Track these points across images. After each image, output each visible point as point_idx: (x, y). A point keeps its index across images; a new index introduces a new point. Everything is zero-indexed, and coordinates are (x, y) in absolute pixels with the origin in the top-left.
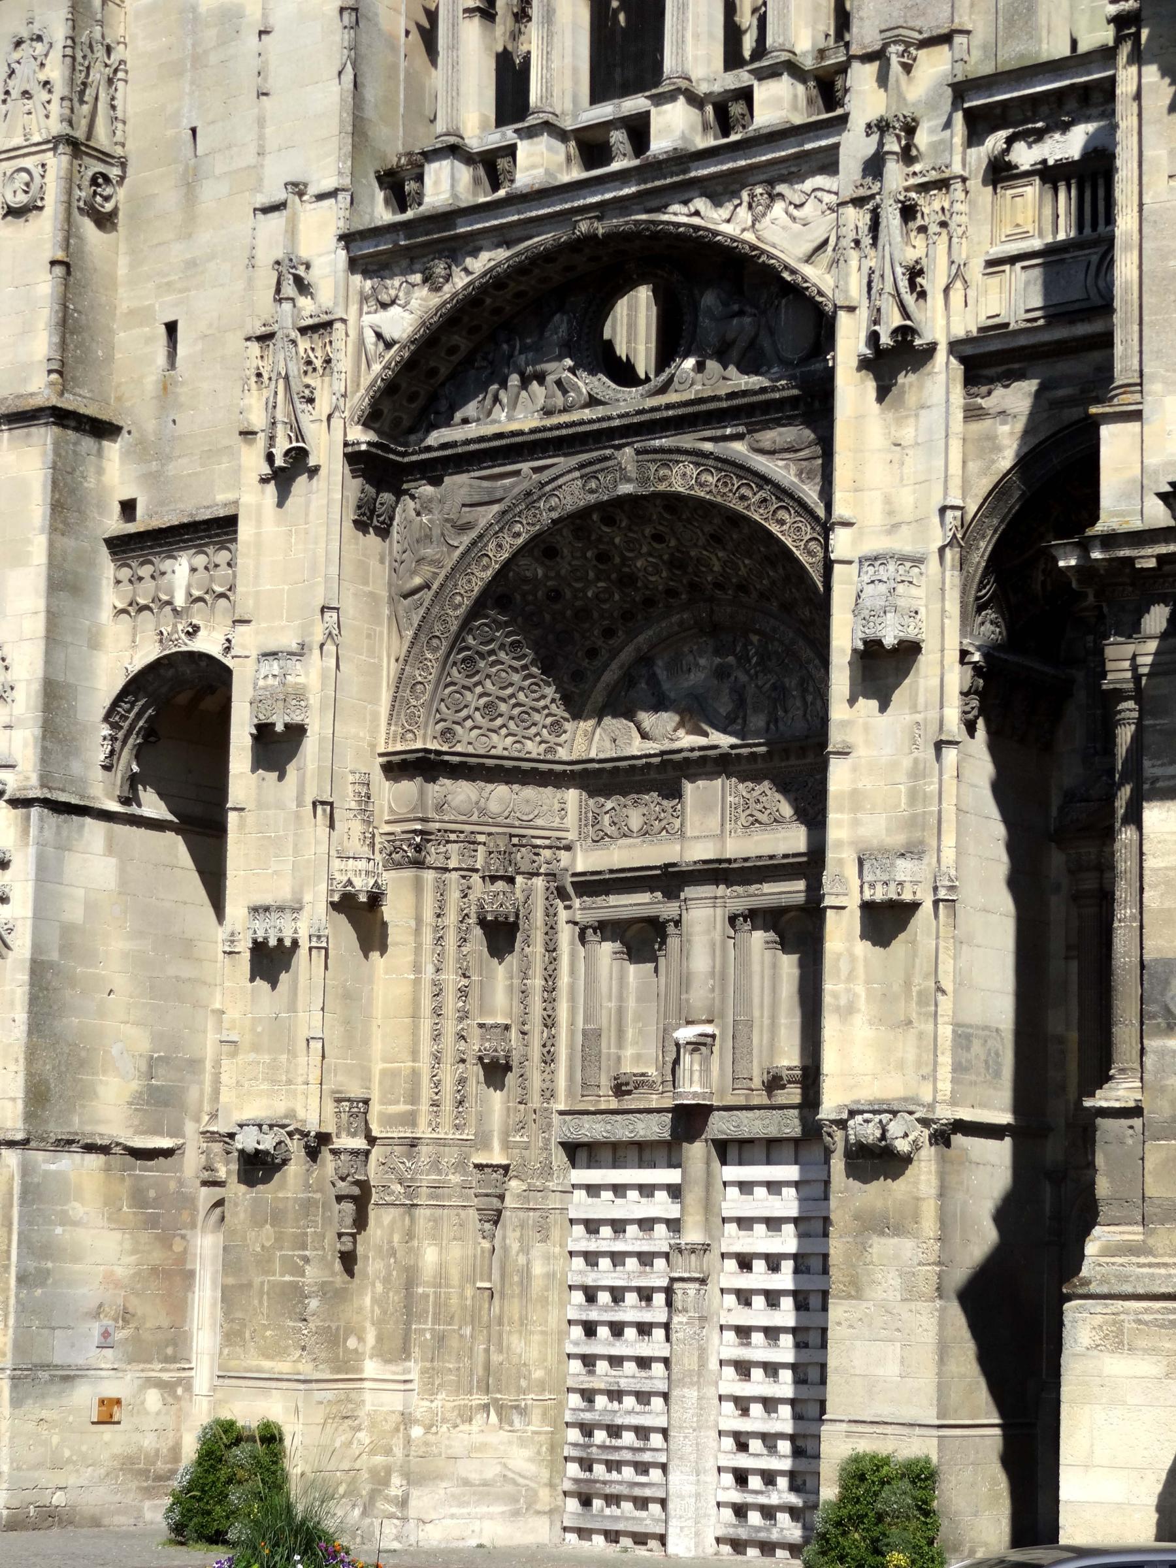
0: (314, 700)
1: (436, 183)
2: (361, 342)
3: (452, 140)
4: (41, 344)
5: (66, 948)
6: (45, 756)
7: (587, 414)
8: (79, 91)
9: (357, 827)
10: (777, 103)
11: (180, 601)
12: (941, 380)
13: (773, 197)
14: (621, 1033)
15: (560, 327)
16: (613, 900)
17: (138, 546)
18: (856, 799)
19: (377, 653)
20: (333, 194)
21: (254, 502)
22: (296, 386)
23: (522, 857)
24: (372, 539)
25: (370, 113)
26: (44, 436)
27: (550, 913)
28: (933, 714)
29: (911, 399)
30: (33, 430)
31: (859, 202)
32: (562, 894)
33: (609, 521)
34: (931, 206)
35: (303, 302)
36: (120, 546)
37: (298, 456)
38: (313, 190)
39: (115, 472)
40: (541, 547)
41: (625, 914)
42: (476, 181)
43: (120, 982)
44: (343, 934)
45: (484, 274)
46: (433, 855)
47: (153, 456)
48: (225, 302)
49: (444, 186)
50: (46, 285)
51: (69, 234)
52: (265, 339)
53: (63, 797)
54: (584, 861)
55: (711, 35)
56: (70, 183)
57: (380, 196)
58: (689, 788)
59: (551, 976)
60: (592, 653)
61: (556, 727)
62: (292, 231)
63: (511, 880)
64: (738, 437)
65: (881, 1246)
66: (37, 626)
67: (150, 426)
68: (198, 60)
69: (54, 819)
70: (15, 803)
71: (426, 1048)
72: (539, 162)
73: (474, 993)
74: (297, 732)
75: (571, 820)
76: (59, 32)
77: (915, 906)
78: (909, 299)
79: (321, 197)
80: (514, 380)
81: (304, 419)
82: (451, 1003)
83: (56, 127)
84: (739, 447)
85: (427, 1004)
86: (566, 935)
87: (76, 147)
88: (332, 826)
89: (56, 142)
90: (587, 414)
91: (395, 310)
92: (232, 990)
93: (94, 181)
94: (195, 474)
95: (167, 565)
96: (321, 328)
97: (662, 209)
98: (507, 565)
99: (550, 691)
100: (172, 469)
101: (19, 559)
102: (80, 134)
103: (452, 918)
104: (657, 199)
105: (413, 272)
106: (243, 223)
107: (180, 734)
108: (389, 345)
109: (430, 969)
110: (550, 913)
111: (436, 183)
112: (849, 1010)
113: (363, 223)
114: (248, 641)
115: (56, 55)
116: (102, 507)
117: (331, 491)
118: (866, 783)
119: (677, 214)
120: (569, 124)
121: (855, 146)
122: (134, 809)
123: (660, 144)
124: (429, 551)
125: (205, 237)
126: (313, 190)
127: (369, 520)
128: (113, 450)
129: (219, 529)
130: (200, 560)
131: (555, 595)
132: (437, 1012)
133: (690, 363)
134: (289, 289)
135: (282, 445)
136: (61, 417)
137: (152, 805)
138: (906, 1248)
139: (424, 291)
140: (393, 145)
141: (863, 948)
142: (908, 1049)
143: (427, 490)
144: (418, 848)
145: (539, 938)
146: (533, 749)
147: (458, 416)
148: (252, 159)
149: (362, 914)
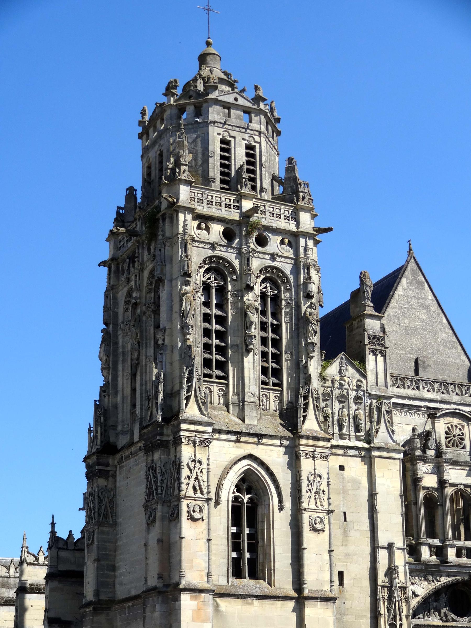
1: (425, 552)
30: (329, 603)
45: (444, 583)
91: (415, 585)
94: (355, 622)
100: (345, 618)
105: (421, 577)
108: (416, 595)
111: (425, 552)
126: (396, 546)
147: (417, 617)
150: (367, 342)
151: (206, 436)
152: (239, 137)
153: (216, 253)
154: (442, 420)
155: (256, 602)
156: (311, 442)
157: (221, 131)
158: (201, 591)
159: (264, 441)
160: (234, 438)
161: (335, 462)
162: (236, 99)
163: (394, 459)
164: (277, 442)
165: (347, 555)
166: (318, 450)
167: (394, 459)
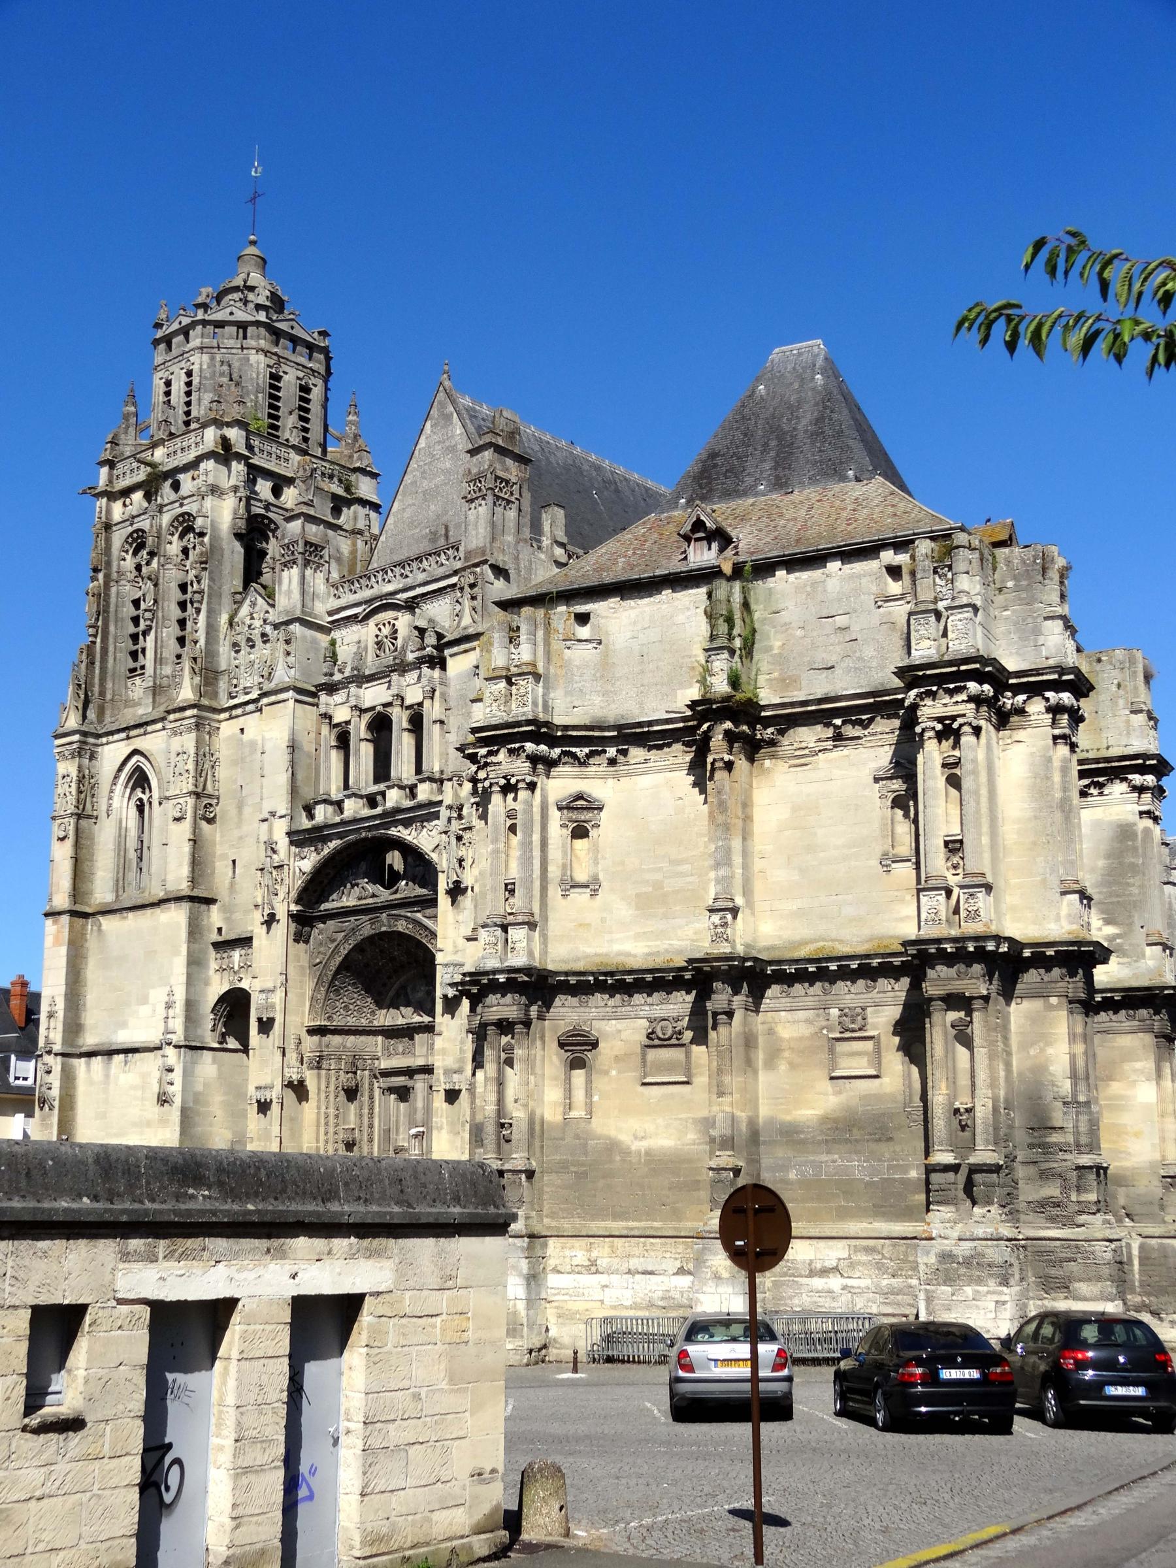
0: (278, 1008)
2: (294, 872)
3: (325, 797)
4: (185, 871)
5: (196, 1100)
6: (186, 1029)
7: (371, 901)
8: (199, 772)
9: (294, 1055)
10: (424, 792)
11: (236, 968)
13: (423, 827)
14: (397, 1130)
15: (363, 866)
16: (393, 1079)
17: (223, 946)
18: (444, 1052)
19: (305, 987)
20: (284, 816)
21: (258, 931)
22: (271, 889)
23: (360, 1063)
24: (302, 945)
25: (299, 783)
26: (186, 906)
27: (371, 1084)
29: (462, 905)
31: (446, 833)
32: (376, 1077)
33: (381, 939)
34: (467, 836)
35: (275, 856)
36: (217, 946)
38: (278, 814)
39: (215, 917)
40: (359, 948)
41: (396, 1085)
42: (335, 811)
43: (219, 1112)
44: (290, 1096)
46: (325, 1064)
47: (227, 910)
48: (251, 855)
49: (322, 814)
50: (187, 848)
51: (195, 827)
52: (262, 870)
53: (194, 1044)
55: (409, 762)
56: (196, 809)
57: (304, 814)
58: (417, 1037)
59: (371, 1108)
60: (384, 985)
61: (373, 1013)
62: (270, 830)
63: (355, 1073)
64: (418, 911)
66: (184, 979)
67: (227, 899)
68: (243, 759)
69: (190, 1052)
70: (176, 1047)
71: (322, 1137)
72: (352, 808)
73: (341, 1116)
74: (271, 1021)
75: (379, 1048)
76: (192, 751)
77: (460, 1091)
78: (458, 870)
79: (281, 817)
80: (349, 886)
81: (274, 902)
82: (332, 1120)
83: (191, 788)
84: (419, 915)
85: (322, 1121)
86: (377, 1092)
87: (198, 795)
88: (284, 1055)
89: (191, 793)
90: (371, 901)
92: (253, 1119)
93: (205, 807)
96: (280, 867)
97: (388, 829)
98: (347, 956)
99: (369, 1000)
100: (234, 917)
101: (177, 953)
102: (199, 790)
103: (332, 1088)
104: (387, 826)
106: (256, 824)
109: (323, 1109)
110: (371, 1084)
112: (440, 1129)
113: (295, 828)
115: (191, 759)
116: (210, 931)
117: (282, 928)
118: (446, 1045)
119: (393, 831)
120: (363, 793)
121: (444, 813)
122: (225, 1046)
123: (390, 804)
124: (322, 949)
125: (246, 828)
126: (278, 814)
127: (299, 937)
128: (214, 908)
129: (245, 942)
130: (243, 952)
131: (367, 965)
132: (326, 1124)
133: (404, 882)
134: (269, 853)
135: (267, 912)
136: (192, 899)
137: (232, 1043)
139: (314, 854)
140: (308, 794)
141: (445, 1105)
142: (458, 1143)
143: (322, 925)
144: (318, 1062)
145: (366, 1094)
146: (364, 1022)
148: (258, 800)
149: (299, 1090)
151: (75, 746)
152: (175, 368)
153: (135, 526)
154: (372, 622)
155: (131, 915)
156: (178, 715)
158: (60, 913)
159: (149, 728)
160: (123, 735)
161: (235, 725)
163: (284, 701)
164: (159, 726)
166: (185, 722)
167: (284, 701)
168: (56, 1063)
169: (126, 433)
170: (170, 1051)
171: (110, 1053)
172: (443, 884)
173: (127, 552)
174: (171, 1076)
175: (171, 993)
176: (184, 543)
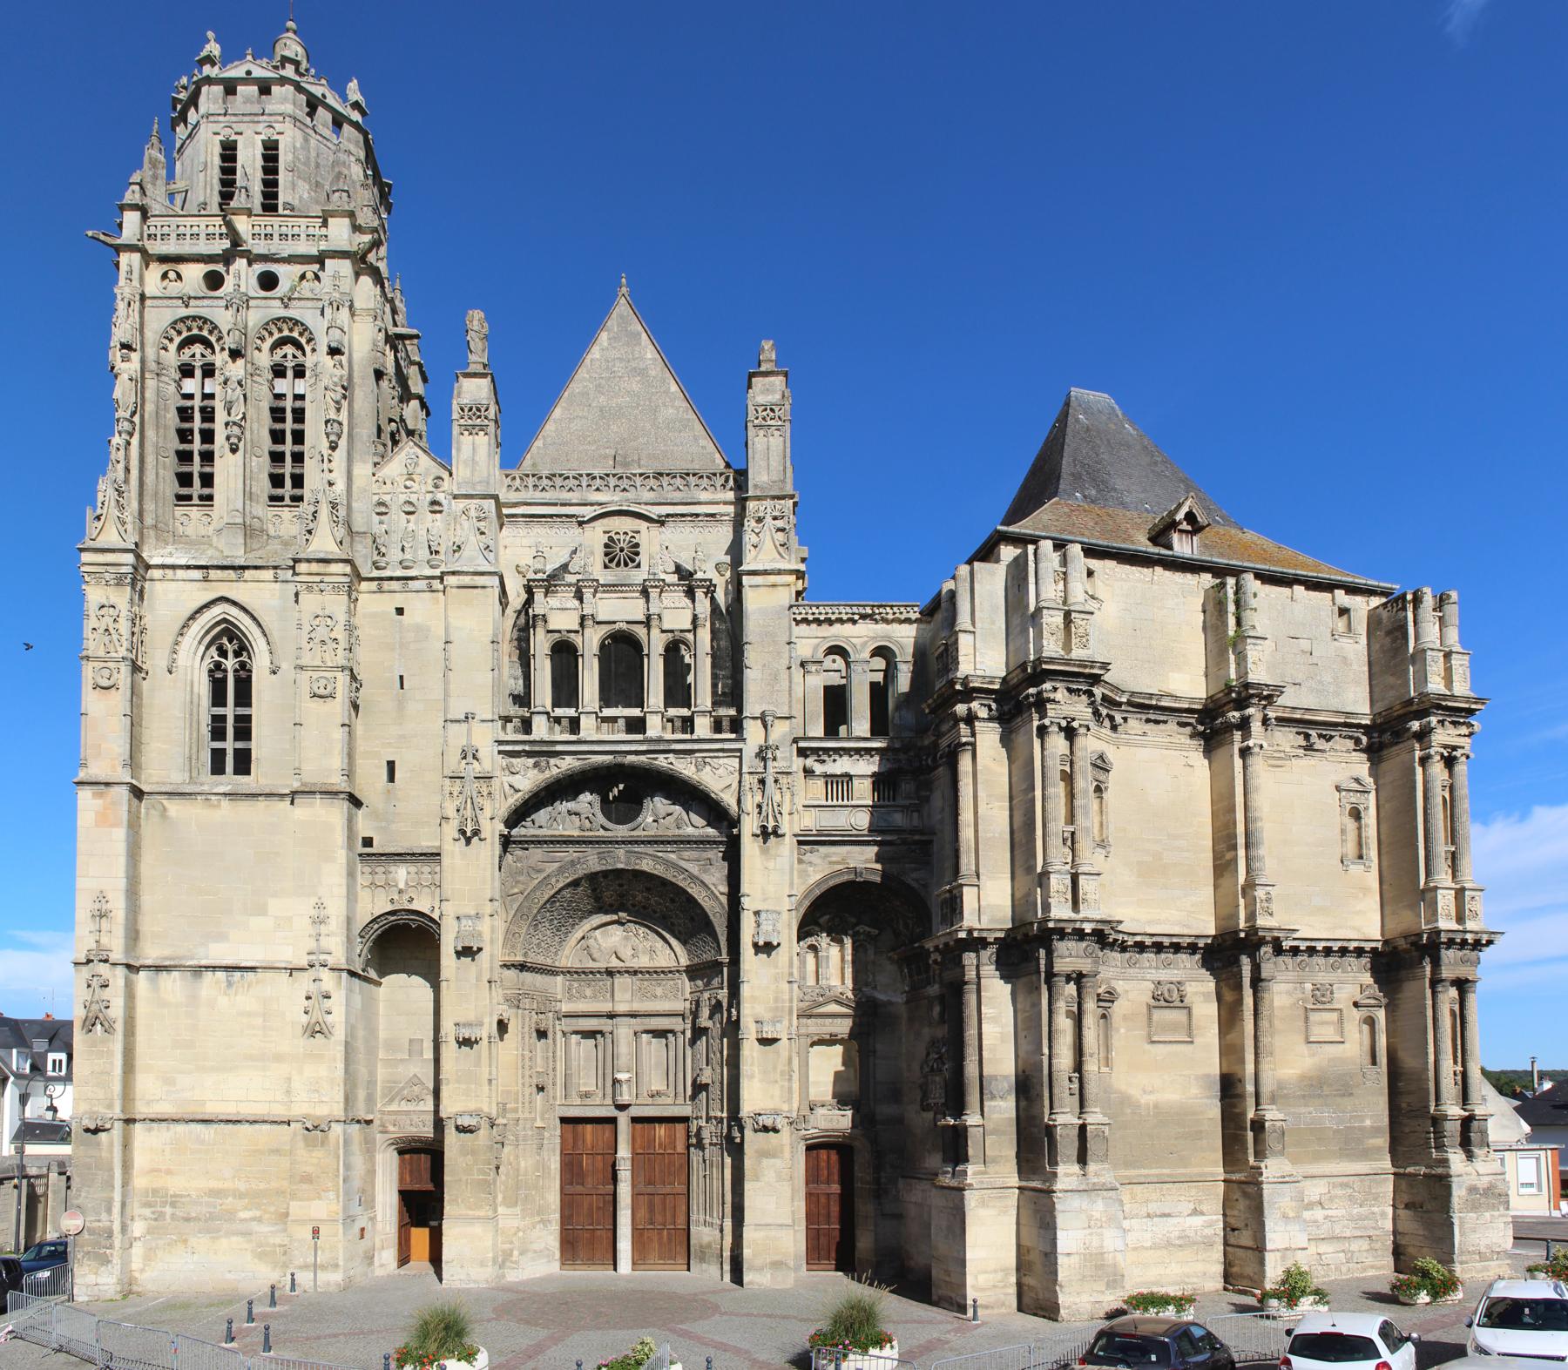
12: (787, 846)
28: (786, 970)
29: (772, 852)
34: (783, 780)
37: (476, 833)
54: (565, 1007)
65: (765, 1162)
95: (392, 868)
100: (393, 827)
107: (403, 944)
108: (517, 791)
112: (752, 1077)
114: (450, 910)
117: (488, 849)
130: (413, 869)
138: (778, 1162)
150: (455, 416)
152: (248, 130)
157: (217, 128)
161: (387, 603)
162: (249, 73)
165: (403, 737)
168: (118, 977)
169: (154, 184)
170: (325, 974)
171: (198, 970)
172: (749, 826)
173: (171, 340)
174: (327, 1004)
175: (320, 906)
176: (277, 357)
